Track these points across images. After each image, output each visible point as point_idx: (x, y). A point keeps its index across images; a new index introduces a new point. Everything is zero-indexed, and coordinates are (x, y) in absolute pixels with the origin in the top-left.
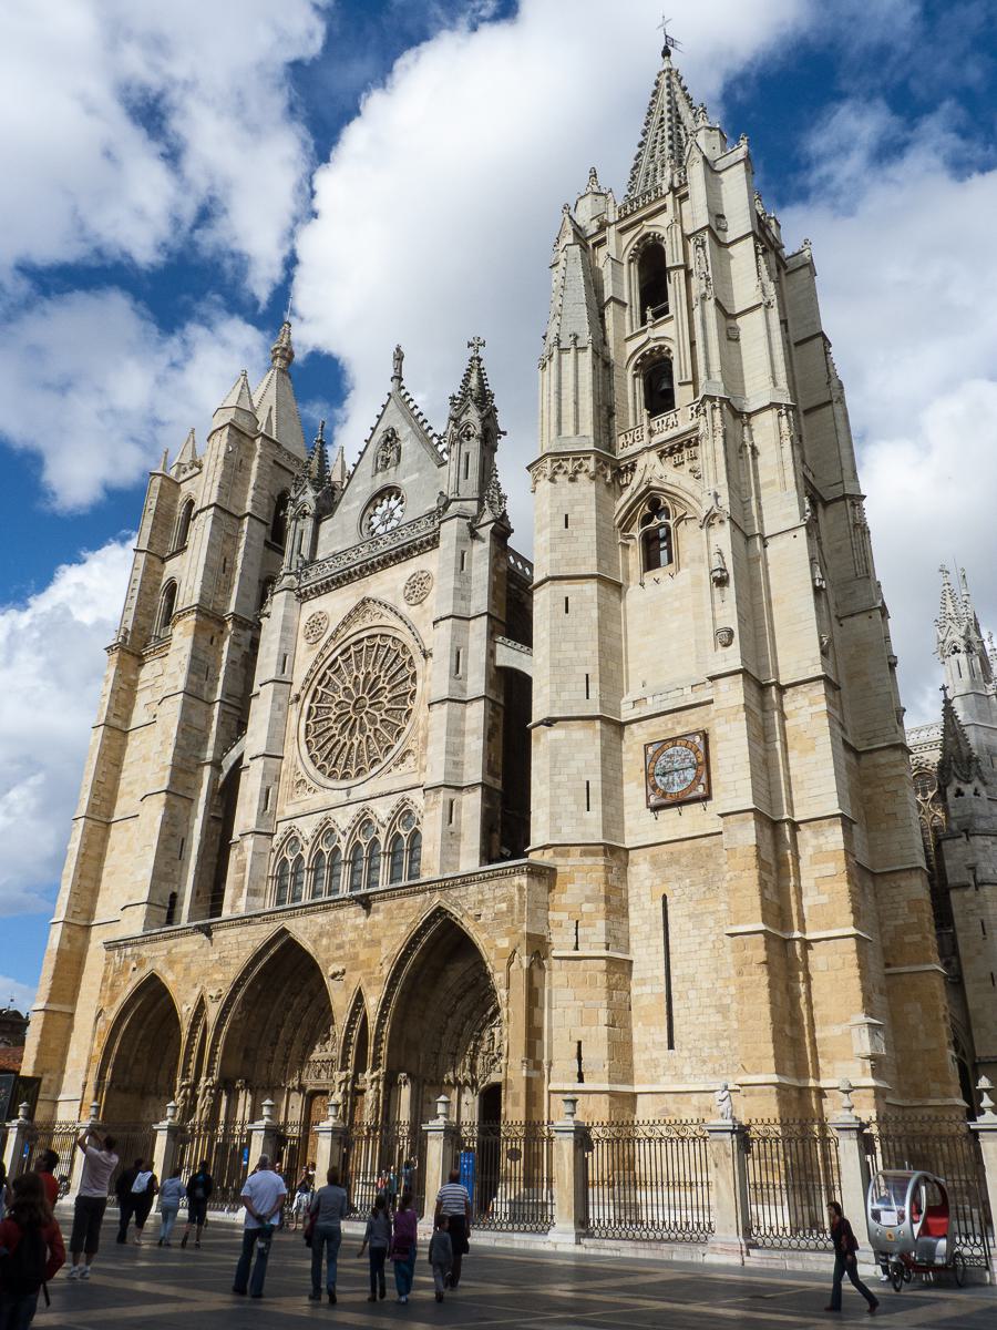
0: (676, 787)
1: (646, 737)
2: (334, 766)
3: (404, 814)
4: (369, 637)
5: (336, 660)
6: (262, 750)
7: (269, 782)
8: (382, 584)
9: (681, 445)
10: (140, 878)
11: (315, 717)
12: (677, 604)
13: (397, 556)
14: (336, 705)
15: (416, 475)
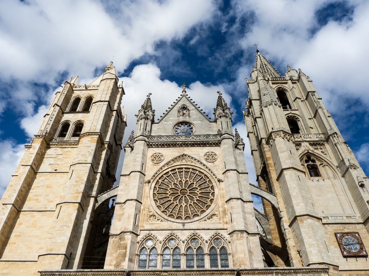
0: (353, 250)
1: (332, 230)
2: (171, 213)
3: (216, 238)
4: (185, 168)
5: (168, 172)
6: (135, 198)
7: (137, 212)
8: (192, 151)
9: (317, 144)
10: (59, 241)
11: (158, 191)
12: (328, 189)
13: (199, 144)
14: (170, 189)
15: (200, 122)
